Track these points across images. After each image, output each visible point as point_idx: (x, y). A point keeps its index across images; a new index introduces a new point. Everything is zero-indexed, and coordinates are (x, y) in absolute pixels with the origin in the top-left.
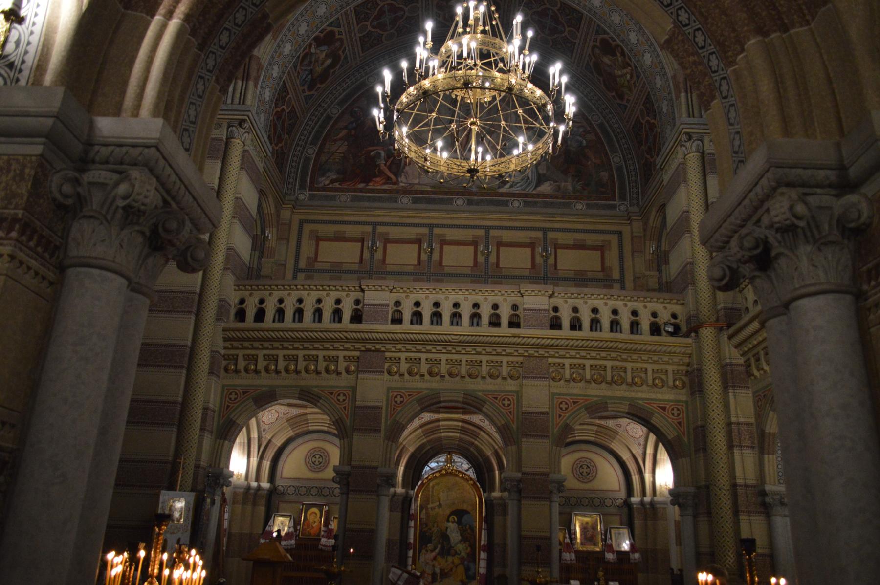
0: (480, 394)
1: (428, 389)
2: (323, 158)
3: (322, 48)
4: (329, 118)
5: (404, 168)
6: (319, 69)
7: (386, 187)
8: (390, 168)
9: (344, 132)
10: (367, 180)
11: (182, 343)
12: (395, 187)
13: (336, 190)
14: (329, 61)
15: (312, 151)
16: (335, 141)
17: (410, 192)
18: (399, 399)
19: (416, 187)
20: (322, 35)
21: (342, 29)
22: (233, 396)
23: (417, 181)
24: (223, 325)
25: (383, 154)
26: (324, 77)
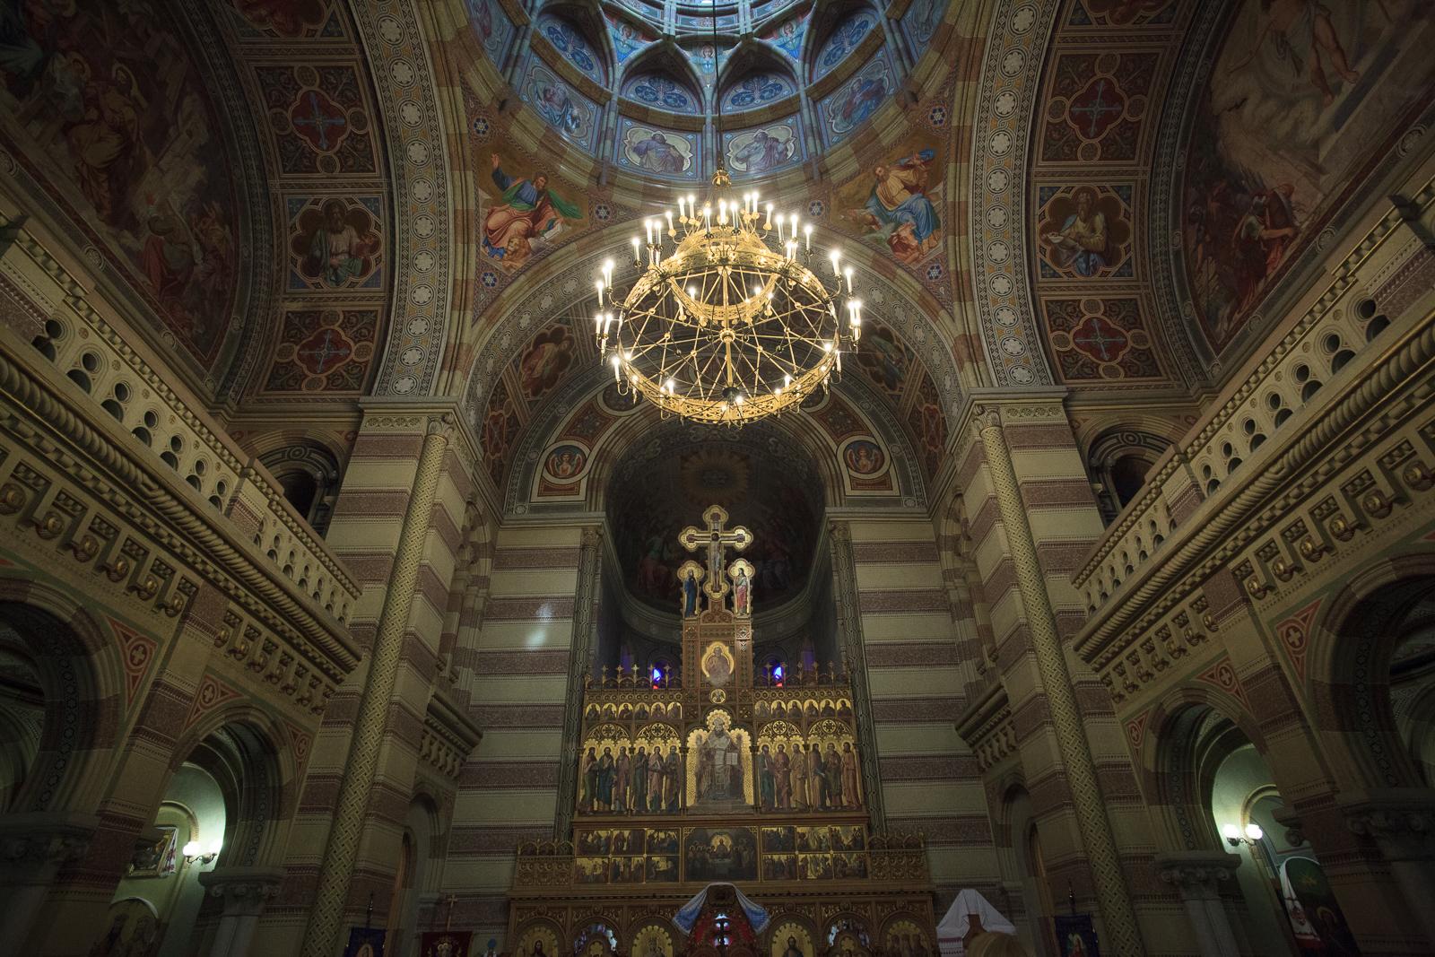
0: (1421, 540)
1: (1322, 590)
2: (1203, 303)
3: (1069, 223)
4: (1177, 254)
5: (1290, 202)
6: (1098, 239)
7: (1288, 253)
8: (1274, 226)
9: (1200, 249)
10: (1261, 274)
11: (1033, 693)
12: (1298, 240)
13: (1241, 322)
14: (1099, 220)
15: (1188, 310)
16: (1200, 271)
17: (1324, 221)
18: (1295, 636)
19: (1325, 206)
20: (1048, 219)
21: (1063, 186)
22: (1134, 735)
23: (1320, 196)
24: (1072, 644)
25: (1252, 219)
26: (1115, 231)
